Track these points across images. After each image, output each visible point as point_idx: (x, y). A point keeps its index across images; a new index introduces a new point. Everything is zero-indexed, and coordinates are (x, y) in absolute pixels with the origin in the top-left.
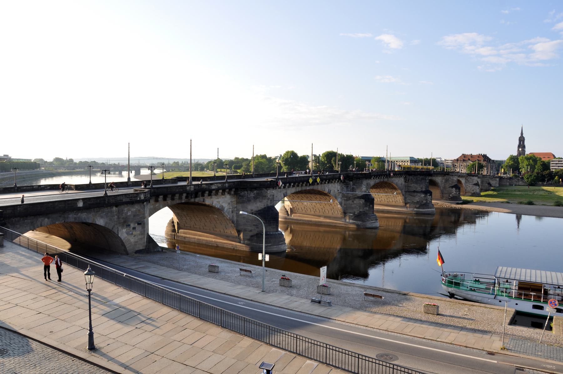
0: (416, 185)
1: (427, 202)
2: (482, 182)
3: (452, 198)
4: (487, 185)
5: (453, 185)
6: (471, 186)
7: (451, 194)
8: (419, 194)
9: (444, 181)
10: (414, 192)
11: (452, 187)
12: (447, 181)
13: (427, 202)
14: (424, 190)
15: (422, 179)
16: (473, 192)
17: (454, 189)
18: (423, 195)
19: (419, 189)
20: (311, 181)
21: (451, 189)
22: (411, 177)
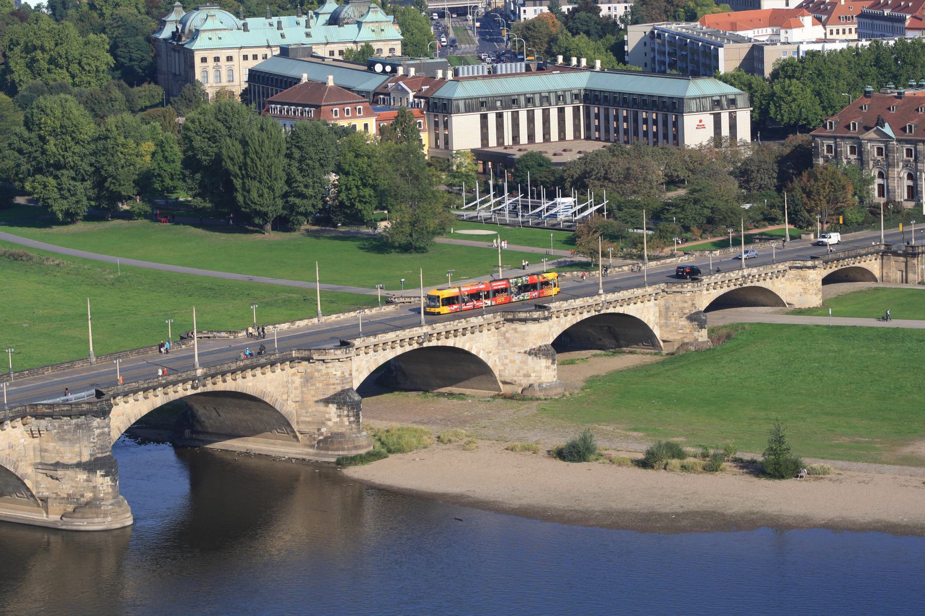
0: (59, 446)
1: (96, 498)
2: (665, 313)
3: (326, 438)
4: (684, 322)
5: (331, 392)
6: (519, 358)
7: (323, 424)
8: (70, 473)
9: (298, 380)
10: (57, 465)
11: (327, 401)
12: (308, 379)
14: (86, 458)
15: (78, 426)
16: (525, 382)
17: (333, 408)
18: (82, 476)
19: (69, 457)
21: (321, 407)
22: (43, 423)
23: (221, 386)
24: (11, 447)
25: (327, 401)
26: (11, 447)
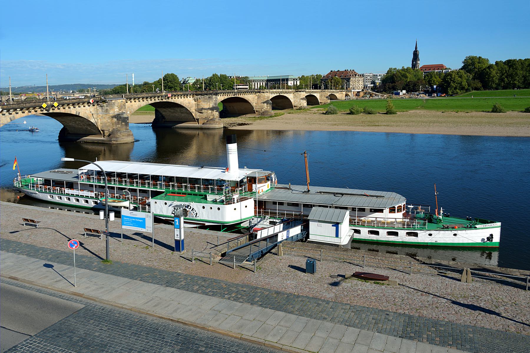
1: (214, 118)
2: (321, 96)
4: (325, 98)
5: (265, 100)
9: (256, 98)
11: (264, 103)
12: (259, 97)
13: (214, 118)
14: (211, 107)
16: (300, 106)
17: (265, 104)
19: (207, 106)
20: (44, 105)
21: (262, 104)
23: (240, 96)
24: (189, 103)
25: (264, 103)
26: (189, 103)
